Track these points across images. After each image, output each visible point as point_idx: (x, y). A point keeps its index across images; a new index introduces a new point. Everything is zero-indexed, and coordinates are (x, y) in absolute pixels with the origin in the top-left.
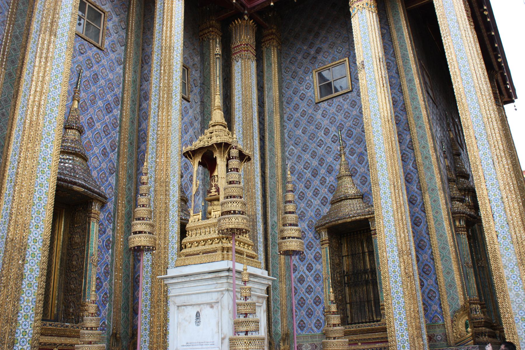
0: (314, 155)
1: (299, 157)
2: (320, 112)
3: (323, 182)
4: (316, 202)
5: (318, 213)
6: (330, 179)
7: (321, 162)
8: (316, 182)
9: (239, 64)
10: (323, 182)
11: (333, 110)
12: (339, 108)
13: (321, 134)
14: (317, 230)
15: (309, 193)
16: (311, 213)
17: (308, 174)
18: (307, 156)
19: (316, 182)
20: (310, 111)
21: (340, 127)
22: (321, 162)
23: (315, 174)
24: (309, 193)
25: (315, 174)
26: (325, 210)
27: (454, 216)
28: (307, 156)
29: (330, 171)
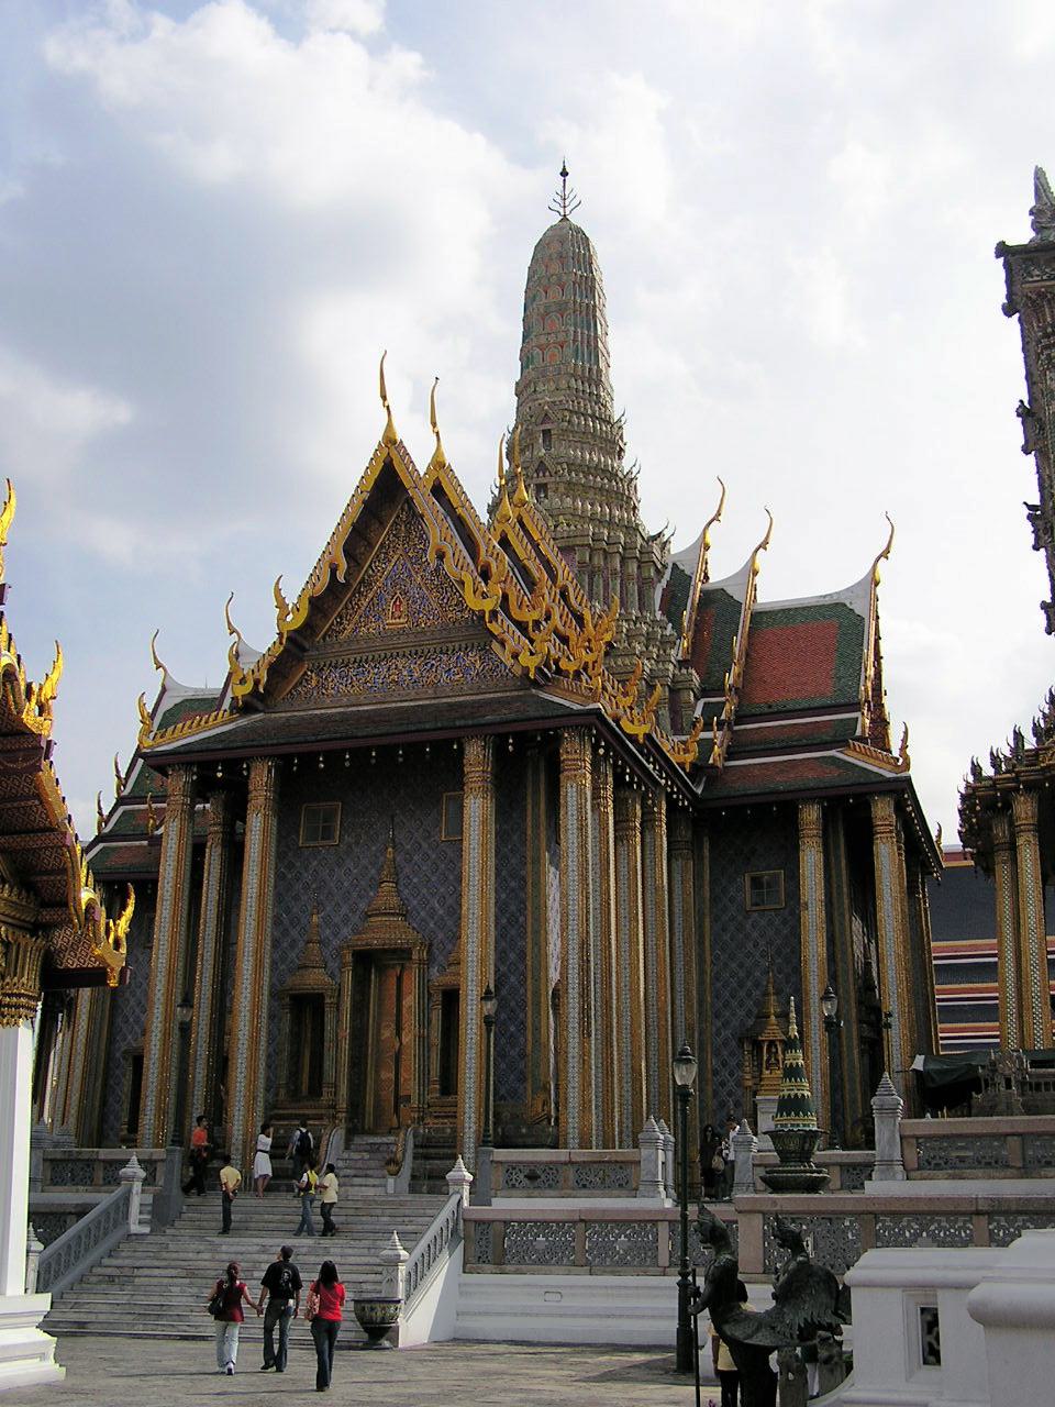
0: (741, 966)
1: (726, 964)
2: (750, 921)
3: (749, 995)
4: (741, 1013)
5: (742, 1023)
6: (756, 993)
7: (749, 974)
8: (742, 994)
9: (679, 863)
10: (749, 995)
11: (763, 923)
12: (770, 923)
13: (750, 945)
14: (741, 1042)
15: (734, 1003)
16: (735, 1023)
17: (734, 983)
18: (734, 965)
19: (742, 994)
20: (740, 918)
21: (770, 943)
22: (749, 974)
23: (741, 985)
24: (734, 1003)
25: (741, 985)
26: (751, 1022)
27: (862, 1040)
28: (734, 965)
29: (757, 985)
